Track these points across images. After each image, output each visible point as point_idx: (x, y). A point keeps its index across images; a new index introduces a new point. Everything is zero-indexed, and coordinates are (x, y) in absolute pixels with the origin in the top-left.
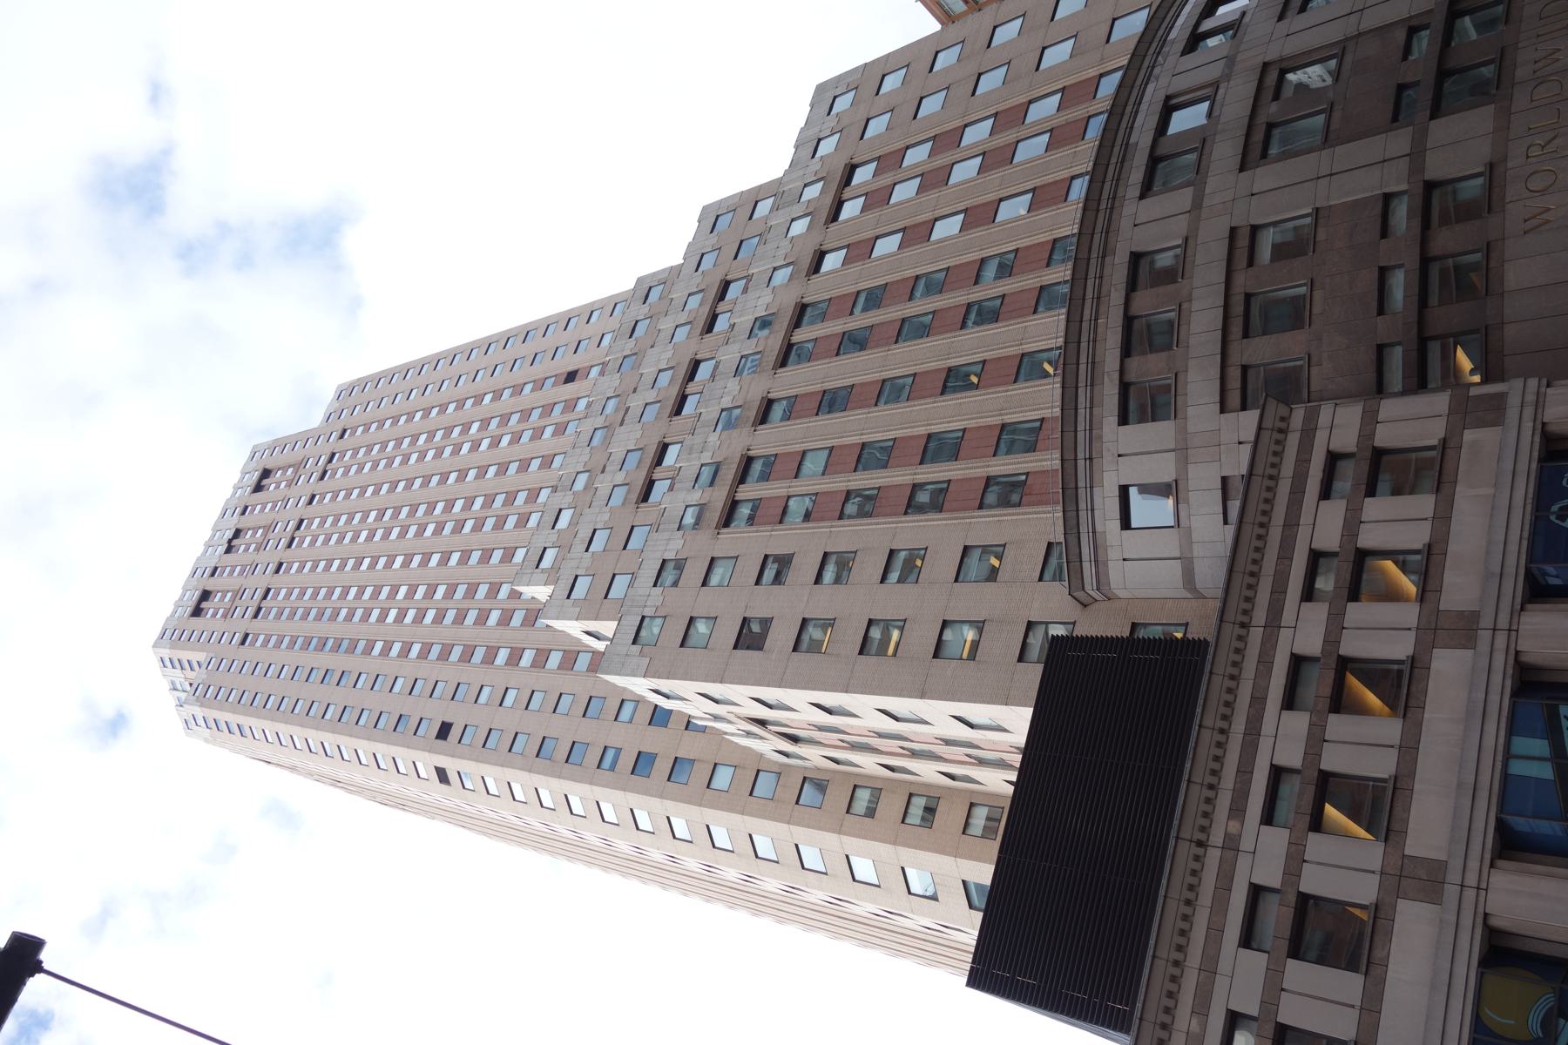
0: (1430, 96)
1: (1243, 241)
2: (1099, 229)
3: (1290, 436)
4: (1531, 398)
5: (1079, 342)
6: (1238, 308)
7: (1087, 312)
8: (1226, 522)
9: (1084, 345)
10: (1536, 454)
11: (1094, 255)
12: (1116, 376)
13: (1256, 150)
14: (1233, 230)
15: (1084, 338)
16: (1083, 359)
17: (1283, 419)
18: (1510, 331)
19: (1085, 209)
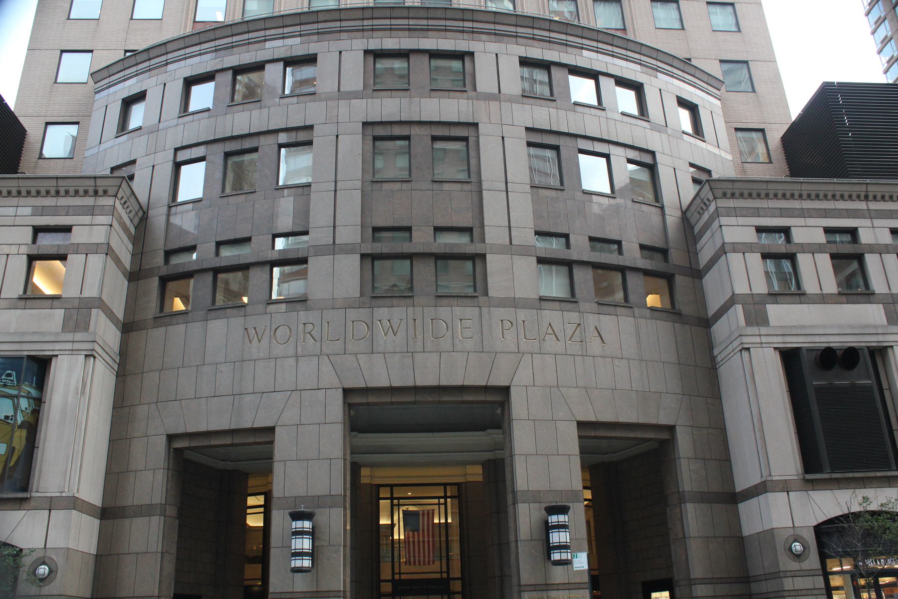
0: (400, 250)
1: (302, 136)
2: (344, 24)
3: (92, 199)
4: (77, 346)
5: (249, 32)
6: (247, 144)
7: (272, 32)
8: (113, 169)
9: (246, 36)
10: (33, 353)
11: (321, 25)
12: (220, 67)
13: (380, 131)
14: (311, 127)
15: (251, 35)
16: (235, 39)
17: (105, 192)
18: (181, 328)
19: (363, 8)
